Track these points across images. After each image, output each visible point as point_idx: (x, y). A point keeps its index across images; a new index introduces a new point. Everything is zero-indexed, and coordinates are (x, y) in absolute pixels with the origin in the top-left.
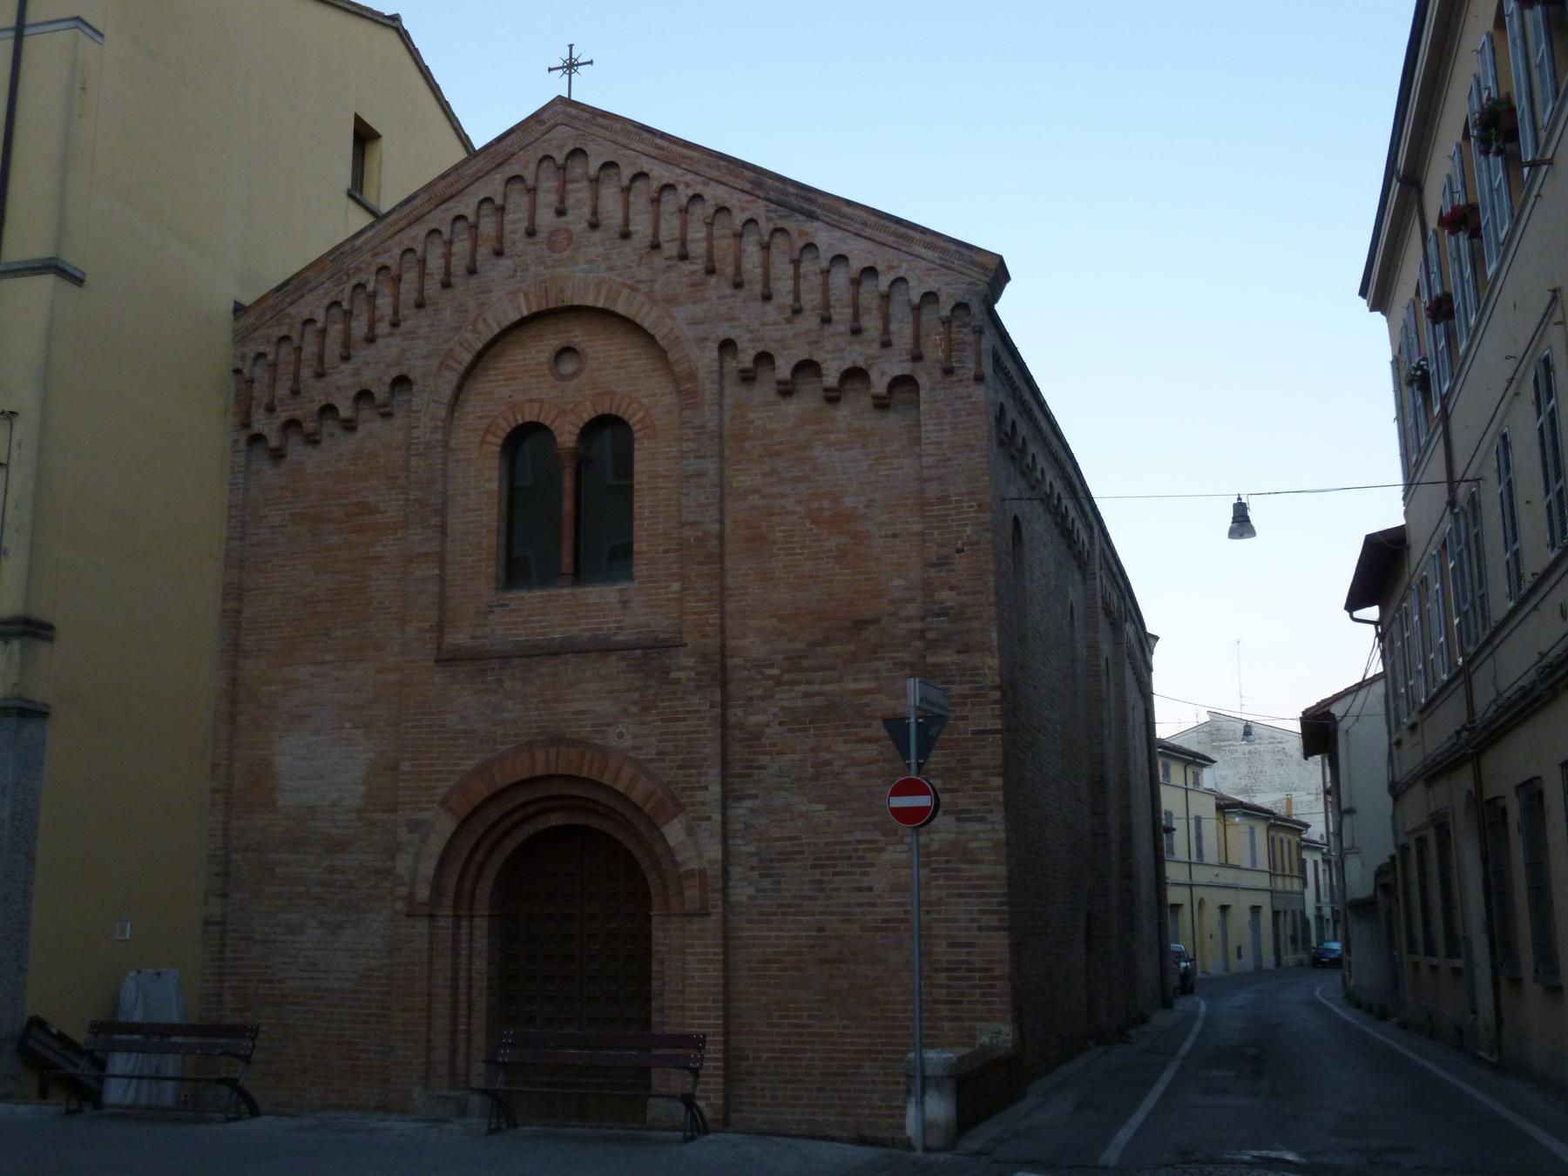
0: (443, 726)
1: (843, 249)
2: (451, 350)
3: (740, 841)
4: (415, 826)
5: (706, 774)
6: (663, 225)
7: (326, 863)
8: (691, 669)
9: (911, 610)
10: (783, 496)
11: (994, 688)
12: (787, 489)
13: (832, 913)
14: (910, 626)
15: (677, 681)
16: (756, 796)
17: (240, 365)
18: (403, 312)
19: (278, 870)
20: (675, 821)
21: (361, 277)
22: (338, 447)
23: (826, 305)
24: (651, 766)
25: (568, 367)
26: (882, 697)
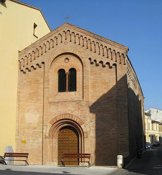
7: (33, 131)
9: (115, 96)
11: (127, 107)
12: (98, 79)
15: (83, 105)
17: (19, 60)
18: (43, 53)
19: (26, 132)
21: (37, 48)
24: (79, 117)
25: (67, 61)
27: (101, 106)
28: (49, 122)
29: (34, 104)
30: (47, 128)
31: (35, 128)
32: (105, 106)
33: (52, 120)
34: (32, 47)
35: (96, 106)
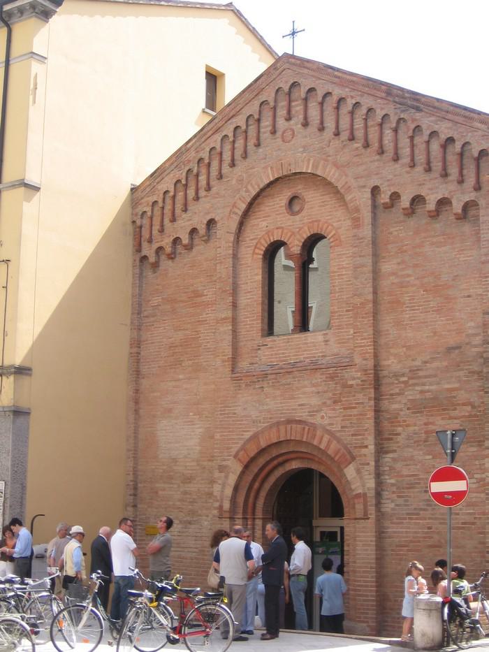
0: (235, 414)
1: (436, 128)
2: (235, 203)
3: (387, 477)
4: (222, 469)
5: (367, 439)
6: (341, 122)
8: (358, 378)
9: (478, 340)
10: (409, 276)
12: (410, 272)
13: (436, 519)
14: (476, 350)
15: (351, 386)
16: (395, 451)
17: (135, 219)
18: (212, 183)
20: (351, 466)
22: (185, 259)
23: (429, 162)
24: (338, 434)
25: (296, 208)
26: (463, 392)
27: (424, 384)
28: (234, 453)
29: (185, 386)
30: (226, 477)
31: (188, 479)
32: (438, 384)
33: (243, 448)
34: (173, 167)
35: (403, 385)
